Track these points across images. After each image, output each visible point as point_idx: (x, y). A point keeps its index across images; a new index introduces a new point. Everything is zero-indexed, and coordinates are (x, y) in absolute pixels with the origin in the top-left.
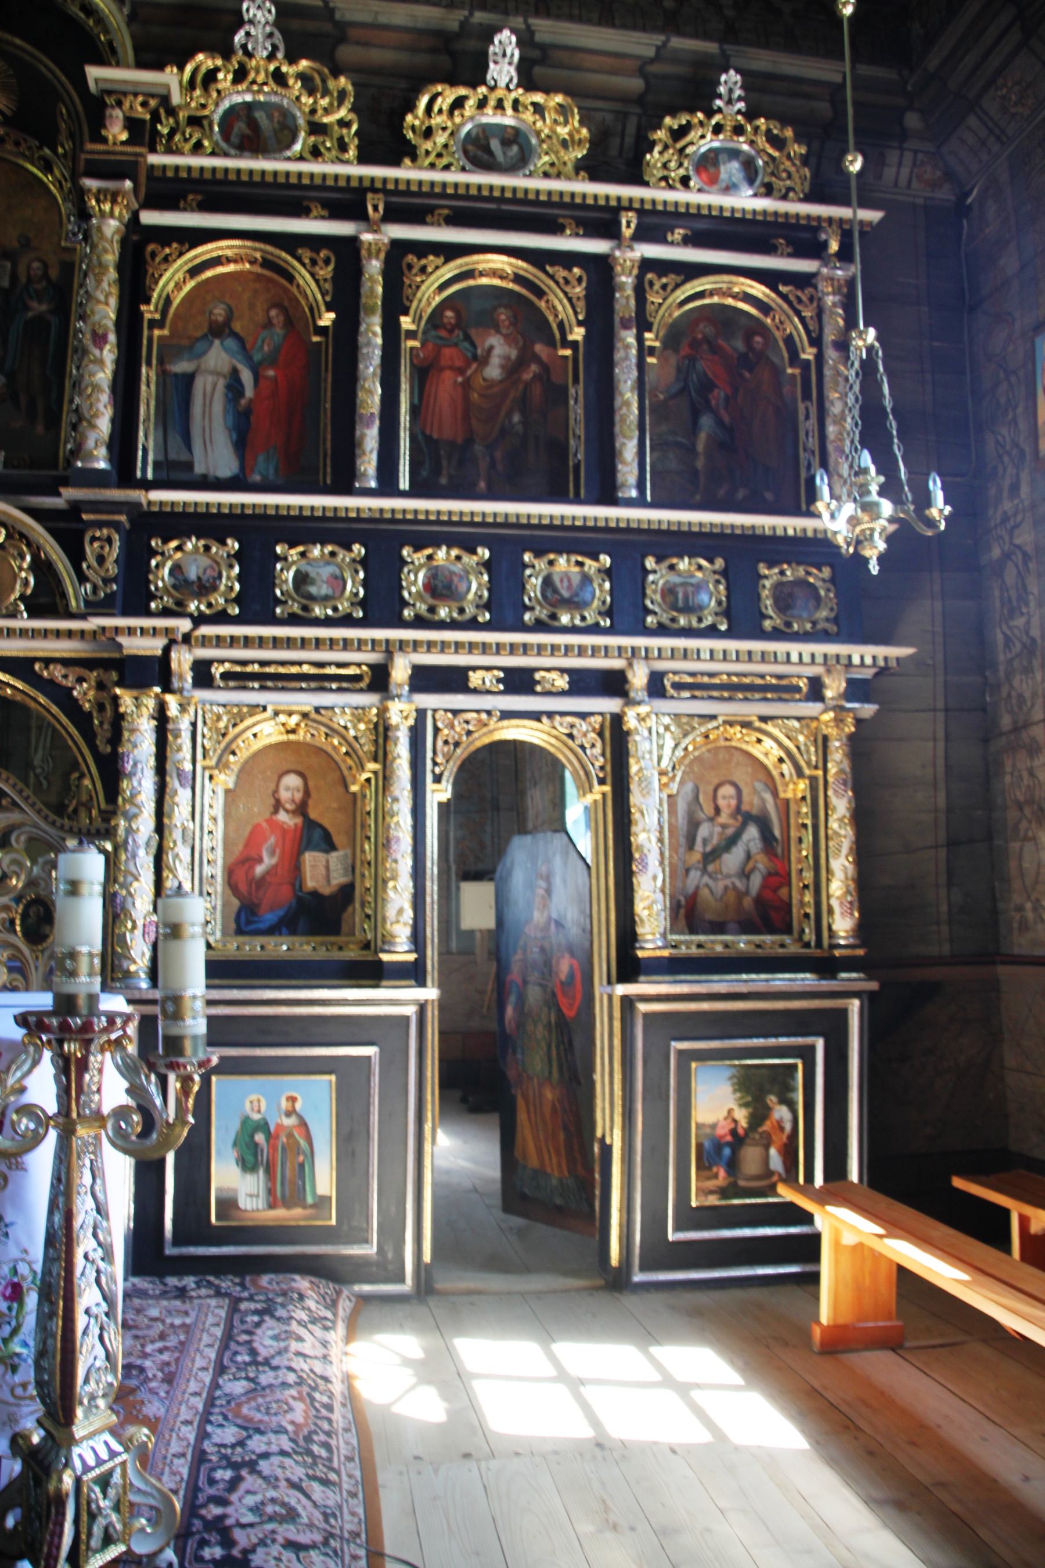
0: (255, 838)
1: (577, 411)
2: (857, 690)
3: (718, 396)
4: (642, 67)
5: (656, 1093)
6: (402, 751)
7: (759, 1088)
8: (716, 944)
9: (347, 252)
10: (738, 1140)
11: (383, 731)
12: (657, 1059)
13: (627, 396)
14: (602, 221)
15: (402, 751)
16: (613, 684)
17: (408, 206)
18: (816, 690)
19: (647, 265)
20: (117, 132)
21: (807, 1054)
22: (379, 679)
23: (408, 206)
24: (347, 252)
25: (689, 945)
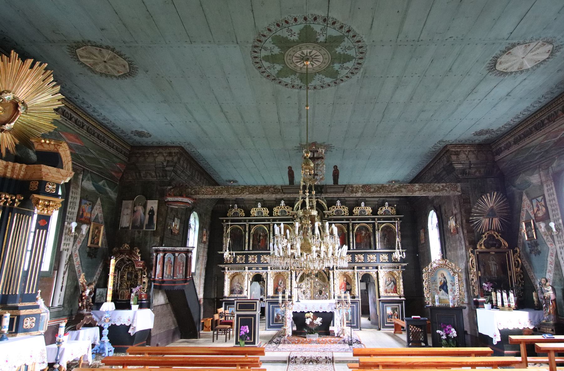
0: (342, 284)
1: (372, 239)
2: (402, 268)
3: (387, 236)
4: (377, 201)
5: (383, 310)
6: (356, 275)
7: (394, 310)
8: (389, 295)
9: (348, 224)
10: (392, 315)
11: (354, 274)
12: (383, 307)
13: (377, 238)
14: (374, 219)
15: (356, 275)
16: (377, 268)
17: (354, 219)
18: (398, 268)
19: (379, 223)
20: (326, 216)
21: (399, 306)
22: (354, 268)
23: (354, 219)
24: (348, 224)
25: (386, 295)
